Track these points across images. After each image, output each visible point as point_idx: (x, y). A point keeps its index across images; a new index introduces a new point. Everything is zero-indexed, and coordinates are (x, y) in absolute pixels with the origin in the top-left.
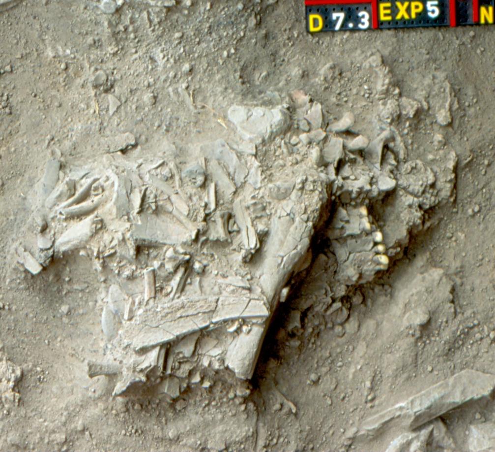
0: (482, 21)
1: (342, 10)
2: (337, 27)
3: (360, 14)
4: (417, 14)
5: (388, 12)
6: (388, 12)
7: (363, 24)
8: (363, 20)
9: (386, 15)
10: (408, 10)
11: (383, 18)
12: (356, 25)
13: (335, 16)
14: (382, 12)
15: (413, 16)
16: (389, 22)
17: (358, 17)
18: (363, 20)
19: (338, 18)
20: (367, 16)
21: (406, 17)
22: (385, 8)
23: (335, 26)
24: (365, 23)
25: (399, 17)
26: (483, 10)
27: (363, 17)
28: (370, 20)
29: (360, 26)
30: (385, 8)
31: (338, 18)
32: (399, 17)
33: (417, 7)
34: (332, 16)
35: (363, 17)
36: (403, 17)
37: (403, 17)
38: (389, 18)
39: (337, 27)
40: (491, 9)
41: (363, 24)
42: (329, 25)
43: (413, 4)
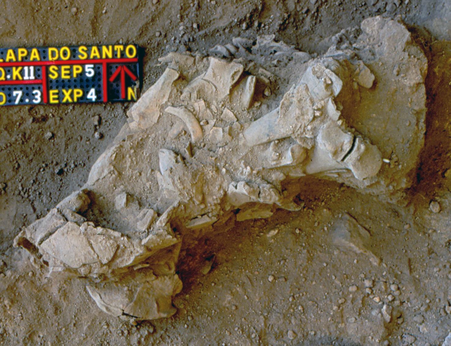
0: (129, 98)
1: (21, 89)
2: (17, 102)
3: (34, 92)
7: (36, 99)
8: (36, 97)
12: (31, 100)
13: (15, 93)
17: (33, 95)
18: (36, 97)
19: (17, 95)
20: (39, 93)
23: (15, 101)
24: (38, 99)
27: (37, 94)
28: (41, 97)
29: (34, 101)
31: (17, 95)
34: (12, 93)
35: (37, 94)
39: (17, 102)
41: (36, 99)
42: (10, 99)
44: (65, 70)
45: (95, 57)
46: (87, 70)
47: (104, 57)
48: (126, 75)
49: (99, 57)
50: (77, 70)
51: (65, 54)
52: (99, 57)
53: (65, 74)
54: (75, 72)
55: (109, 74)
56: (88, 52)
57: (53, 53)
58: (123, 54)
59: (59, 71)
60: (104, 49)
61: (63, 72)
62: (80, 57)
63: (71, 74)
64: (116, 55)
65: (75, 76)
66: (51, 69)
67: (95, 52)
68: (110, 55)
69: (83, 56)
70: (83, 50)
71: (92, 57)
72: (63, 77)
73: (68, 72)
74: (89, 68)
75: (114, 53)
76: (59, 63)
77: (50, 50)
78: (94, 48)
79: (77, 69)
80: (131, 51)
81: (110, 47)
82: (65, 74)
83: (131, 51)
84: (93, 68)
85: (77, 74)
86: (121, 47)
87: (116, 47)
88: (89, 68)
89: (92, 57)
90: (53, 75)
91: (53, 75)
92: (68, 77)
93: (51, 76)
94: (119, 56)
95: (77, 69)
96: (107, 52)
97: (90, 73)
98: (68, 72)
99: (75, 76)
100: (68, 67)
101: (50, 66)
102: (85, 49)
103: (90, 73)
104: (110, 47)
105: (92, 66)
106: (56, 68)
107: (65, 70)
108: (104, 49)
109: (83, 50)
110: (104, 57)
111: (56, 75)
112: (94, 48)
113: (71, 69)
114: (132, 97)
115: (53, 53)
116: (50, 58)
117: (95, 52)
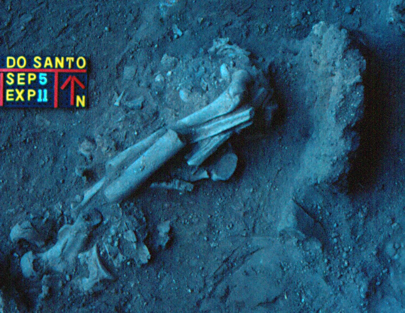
0: (78, 105)
4: (31, 98)
5: (12, 95)
6: (12, 95)
9: (10, 97)
10: (25, 95)
11: (8, 99)
14: (8, 95)
15: (29, 99)
16: (13, 103)
21: (22, 99)
22: (10, 93)
25: (17, 99)
26: (78, 98)
30: (10, 93)
32: (17, 99)
33: (32, 93)
36: (20, 100)
37: (20, 100)
38: (12, 99)
40: (84, 97)
43: (29, 91)
44: (21, 77)
45: (48, 67)
46: (41, 78)
47: (56, 66)
48: (76, 84)
49: (51, 66)
50: (31, 78)
51: (21, 62)
52: (51, 66)
53: (21, 81)
54: (30, 80)
55: (60, 83)
56: (43, 62)
57: (11, 62)
58: (74, 64)
59: (15, 79)
60: (57, 60)
61: (19, 79)
62: (35, 66)
63: (26, 81)
64: (68, 66)
65: (29, 83)
66: (8, 76)
67: (48, 62)
68: (62, 65)
69: (37, 65)
70: (38, 60)
71: (45, 66)
72: (19, 83)
73: (23, 79)
74: (42, 76)
75: (66, 64)
76: (16, 71)
77: (8, 58)
78: (48, 59)
79: (32, 77)
80: (81, 63)
81: (63, 59)
82: (21, 81)
83: (81, 63)
84: (47, 77)
85: (32, 82)
86: (72, 59)
87: (68, 59)
88: (42, 76)
89: (45, 66)
90: (10, 81)
91: (10, 81)
92: (23, 84)
93: (7, 82)
94: (70, 66)
95: (32, 77)
96: (60, 62)
97: (43, 81)
98: (23, 79)
99: (29, 83)
100: (23, 74)
101: (7, 73)
102: (40, 59)
103: (43, 81)
104: (63, 59)
105: (45, 75)
106: (13, 75)
107: (21, 77)
108: (57, 60)
109: (38, 60)
110: (56, 66)
111: (13, 81)
112: (48, 59)
113: (26, 77)
114: (80, 104)
115: (11, 62)
116: (8, 66)
117: (48, 62)
